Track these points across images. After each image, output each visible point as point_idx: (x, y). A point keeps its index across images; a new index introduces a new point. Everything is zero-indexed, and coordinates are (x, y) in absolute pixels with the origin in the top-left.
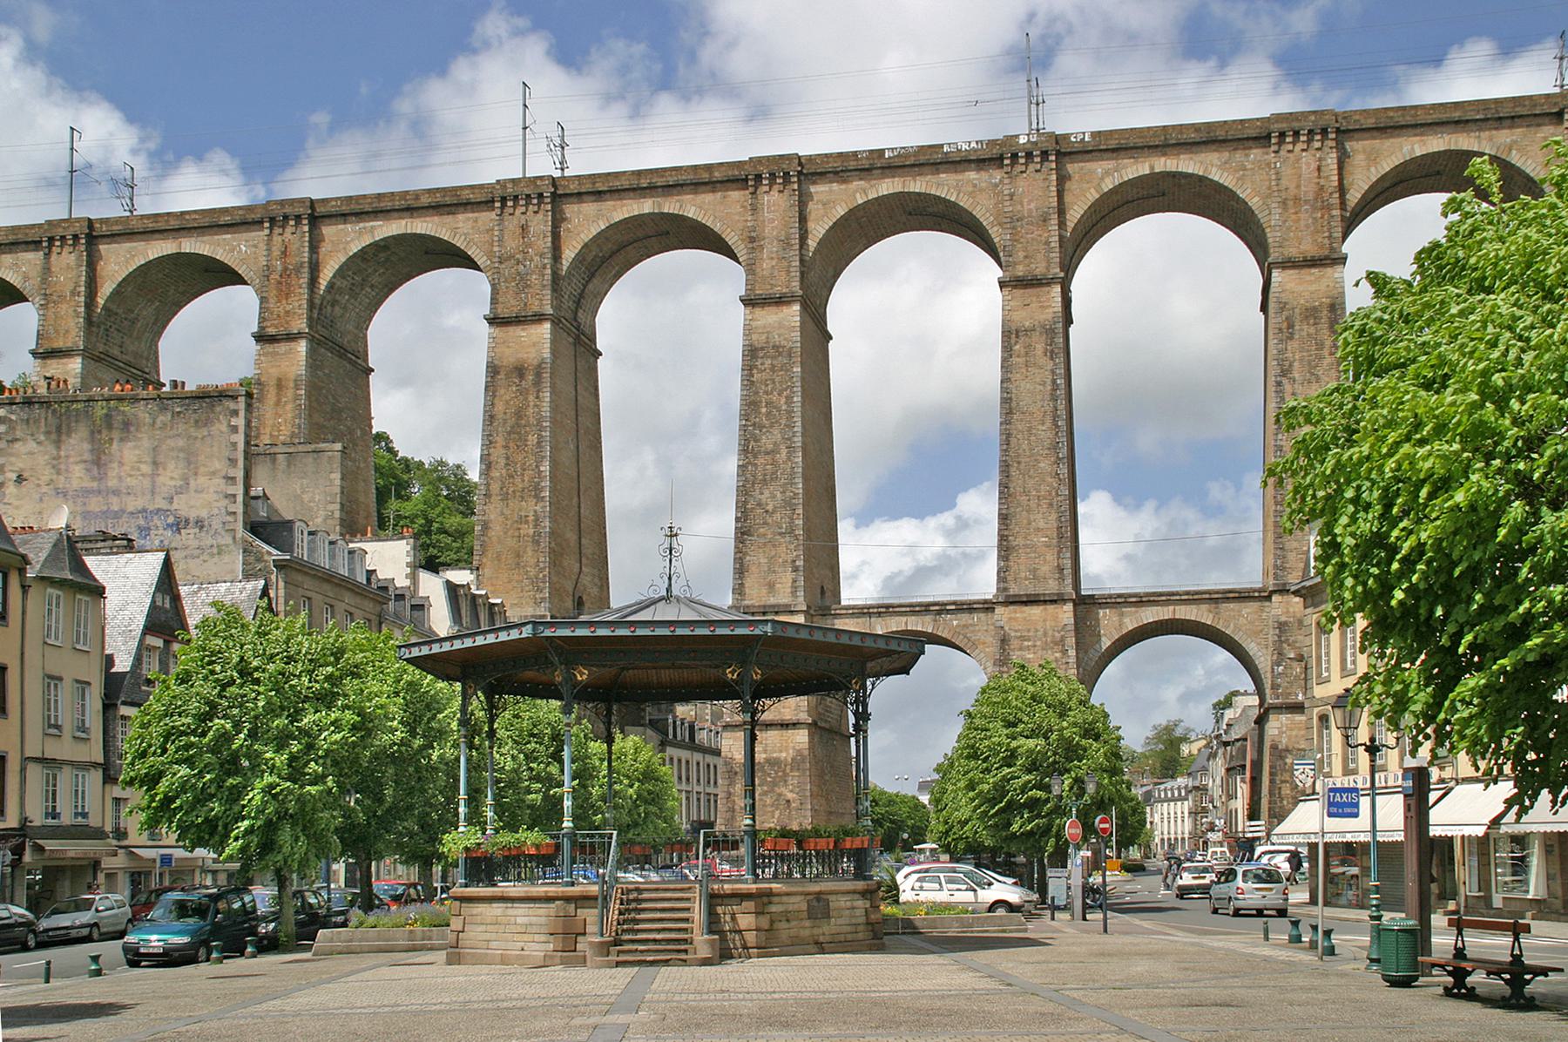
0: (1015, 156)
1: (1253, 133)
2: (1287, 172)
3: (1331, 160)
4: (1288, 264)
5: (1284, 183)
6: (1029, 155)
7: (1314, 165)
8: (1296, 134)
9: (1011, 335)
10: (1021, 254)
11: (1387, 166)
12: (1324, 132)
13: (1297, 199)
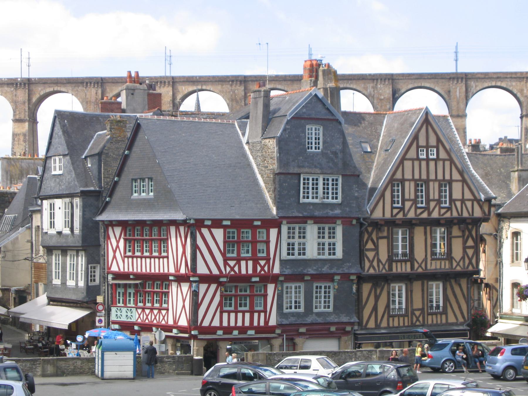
0: (17, 84)
1: (80, 81)
2: (88, 94)
3: (100, 91)
5: (87, 96)
6: (21, 84)
7: (95, 92)
8: (91, 83)
9: (14, 135)
10: (18, 112)
12: (98, 83)
13: (90, 101)
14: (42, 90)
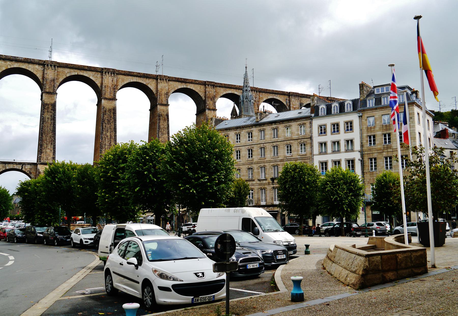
0: (48, 65)
3: (115, 79)
4: (106, 99)
5: (105, 82)
7: (111, 80)
8: (108, 73)
10: (48, 87)
11: (125, 83)
12: (114, 74)
14: (68, 73)
